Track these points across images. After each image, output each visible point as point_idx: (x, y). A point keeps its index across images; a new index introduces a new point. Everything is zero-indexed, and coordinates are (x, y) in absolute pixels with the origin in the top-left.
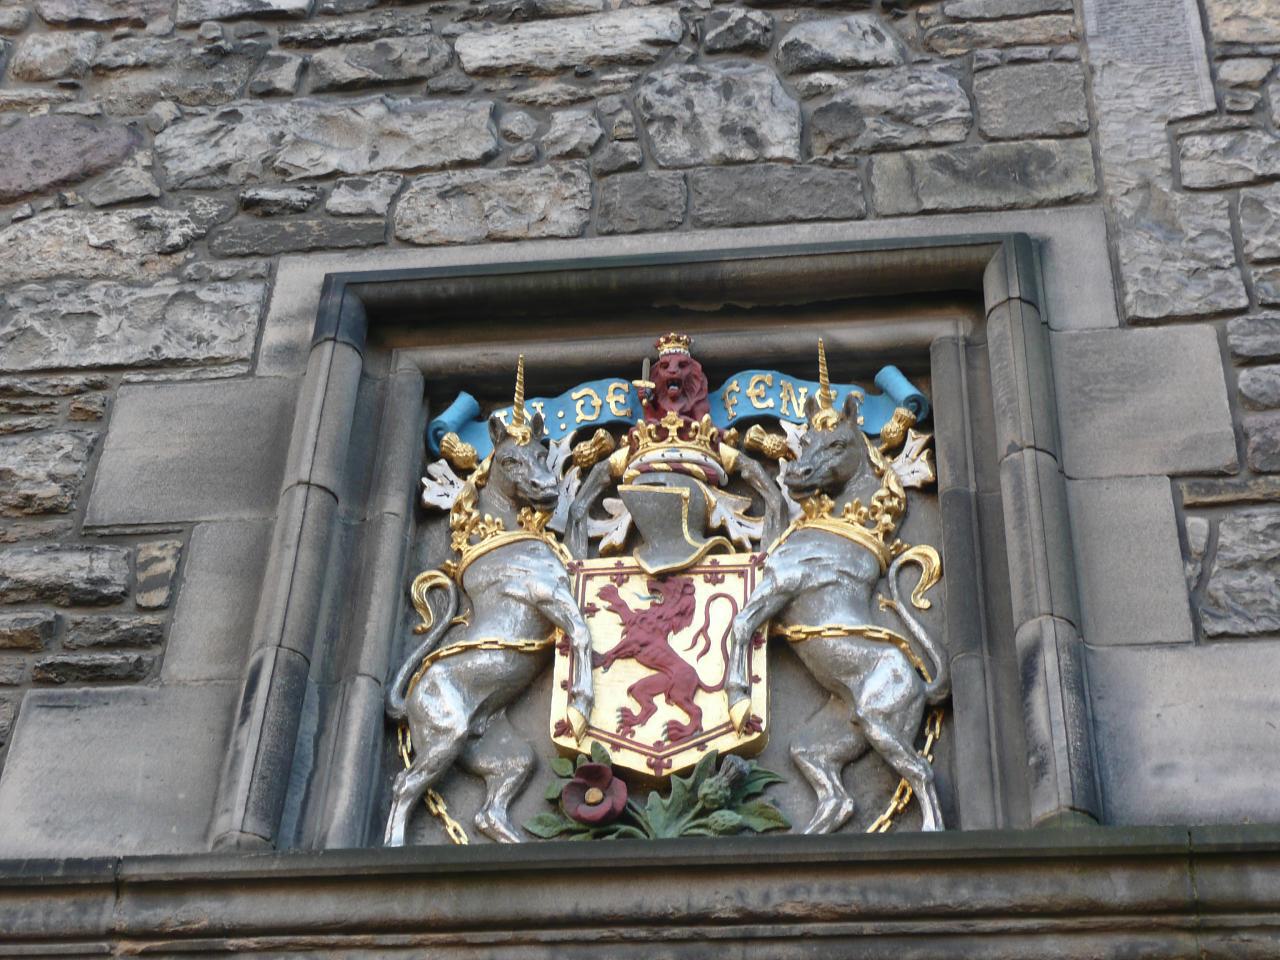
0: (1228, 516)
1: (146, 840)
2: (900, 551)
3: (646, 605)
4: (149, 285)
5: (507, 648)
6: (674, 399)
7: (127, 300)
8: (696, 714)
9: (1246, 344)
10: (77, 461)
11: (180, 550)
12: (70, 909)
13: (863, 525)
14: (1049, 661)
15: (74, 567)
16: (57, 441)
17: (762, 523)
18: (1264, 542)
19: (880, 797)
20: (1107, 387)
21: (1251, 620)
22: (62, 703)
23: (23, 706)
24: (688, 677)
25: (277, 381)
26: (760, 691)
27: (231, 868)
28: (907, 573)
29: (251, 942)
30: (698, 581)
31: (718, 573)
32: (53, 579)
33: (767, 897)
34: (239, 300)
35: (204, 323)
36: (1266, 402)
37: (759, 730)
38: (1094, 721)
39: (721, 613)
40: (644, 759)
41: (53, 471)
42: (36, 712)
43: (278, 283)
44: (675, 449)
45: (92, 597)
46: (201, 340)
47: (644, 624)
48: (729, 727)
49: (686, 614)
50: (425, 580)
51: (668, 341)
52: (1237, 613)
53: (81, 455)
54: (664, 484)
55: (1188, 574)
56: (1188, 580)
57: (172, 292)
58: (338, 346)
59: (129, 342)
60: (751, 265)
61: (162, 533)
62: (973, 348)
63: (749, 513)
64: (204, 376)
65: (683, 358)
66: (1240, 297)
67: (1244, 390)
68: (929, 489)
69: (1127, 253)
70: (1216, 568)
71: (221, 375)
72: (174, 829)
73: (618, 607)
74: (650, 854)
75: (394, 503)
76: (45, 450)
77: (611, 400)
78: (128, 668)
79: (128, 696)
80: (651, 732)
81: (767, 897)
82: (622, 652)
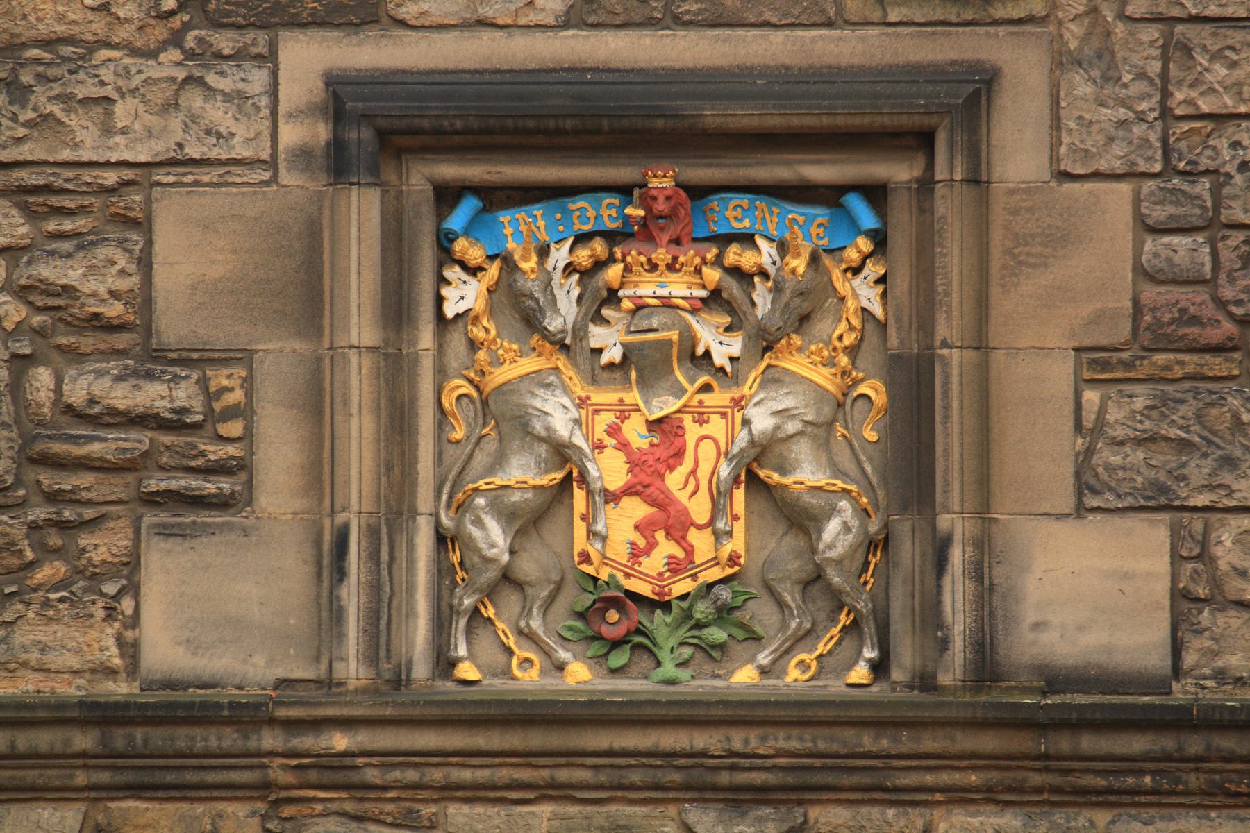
0: (1112, 391)
1: (271, 661)
2: (856, 383)
3: (644, 444)
4: (152, 54)
5: (534, 487)
6: (662, 229)
7: (136, 81)
8: (689, 551)
9: (1155, 214)
10: (130, 275)
11: (244, 380)
12: (236, 735)
13: (824, 365)
14: (958, 556)
15: (153, 396)
16: (110, 256)
17: (740, 338)
18: (1141, 422)
19: (832, 611)
20: (1033, 251)
21: (1119, 496)
22: (175, 531)
23: (143, 531)
24: (683, 518)
25: (299, 192)
26: (739, 528)
27: (356, 713)
28: (860, 403)
29: (374, 760)
30: (688, 421)
31: (703, 413)
32: (142, 409)
33: (746, 742)
34: (249, 89)
35: (218, 114)
36: (1162, 278)
37: (739, 565)
38: (991, 584)
39: (707, 449)
40: (650, 587)
41: (113, 288)
42: (157, 538)
43: (281, 66)
44: (663, 286)
45: (176, 423)
46: (219, 136)
47: (645, 468)
48: (716, 561)
49: (679, 454)
50: (453, 390)
51: (655, 176)
52: (1111, 489)
53: (132, 268)
54: (656, 330)
55: (1077, 448)
56: (1077, 455)
57: (181, 74)
58: (362, 189)
59: (150, 134)
60: (729, 119)
61: (225, 359)
62: (926, 185)
63: (728, 329)
64: (231, 180)
65: (666, 193)
66: (1156, 161)
67: (1145, 264)
68: (883, 326)
69: (1066, 95)
70: (1100, 445)
71: (245, 179)
72: (292, 651)
73: (624, 446)
74: (664, 712)
75: (426, 338)
76: (100, 264)
77: (605, 213)
78: (224, 499)
79: (229, 527)
80: (654, 563)
81: (746, 742)
82: (628, 491)
